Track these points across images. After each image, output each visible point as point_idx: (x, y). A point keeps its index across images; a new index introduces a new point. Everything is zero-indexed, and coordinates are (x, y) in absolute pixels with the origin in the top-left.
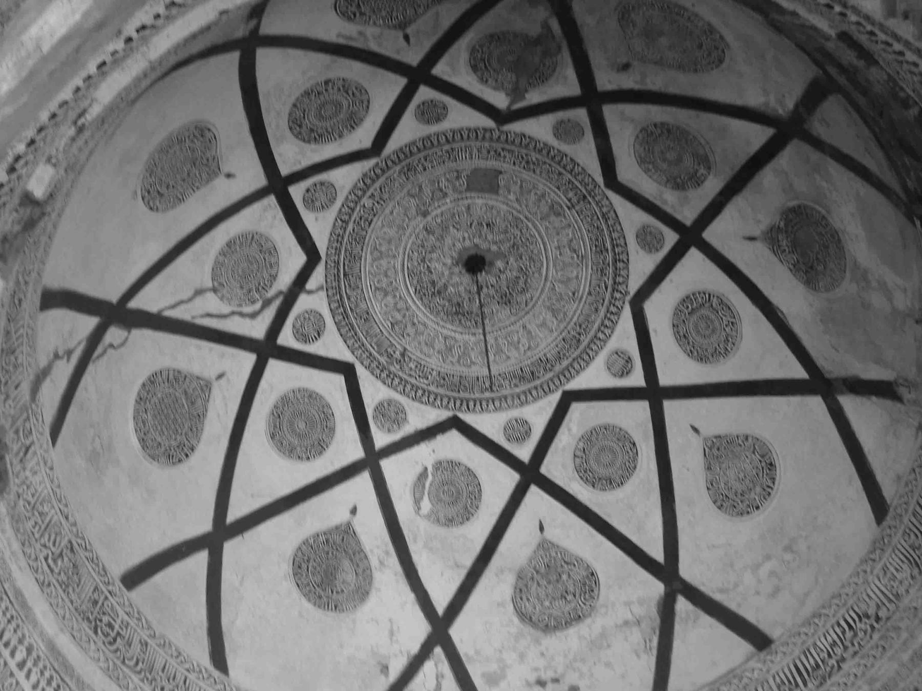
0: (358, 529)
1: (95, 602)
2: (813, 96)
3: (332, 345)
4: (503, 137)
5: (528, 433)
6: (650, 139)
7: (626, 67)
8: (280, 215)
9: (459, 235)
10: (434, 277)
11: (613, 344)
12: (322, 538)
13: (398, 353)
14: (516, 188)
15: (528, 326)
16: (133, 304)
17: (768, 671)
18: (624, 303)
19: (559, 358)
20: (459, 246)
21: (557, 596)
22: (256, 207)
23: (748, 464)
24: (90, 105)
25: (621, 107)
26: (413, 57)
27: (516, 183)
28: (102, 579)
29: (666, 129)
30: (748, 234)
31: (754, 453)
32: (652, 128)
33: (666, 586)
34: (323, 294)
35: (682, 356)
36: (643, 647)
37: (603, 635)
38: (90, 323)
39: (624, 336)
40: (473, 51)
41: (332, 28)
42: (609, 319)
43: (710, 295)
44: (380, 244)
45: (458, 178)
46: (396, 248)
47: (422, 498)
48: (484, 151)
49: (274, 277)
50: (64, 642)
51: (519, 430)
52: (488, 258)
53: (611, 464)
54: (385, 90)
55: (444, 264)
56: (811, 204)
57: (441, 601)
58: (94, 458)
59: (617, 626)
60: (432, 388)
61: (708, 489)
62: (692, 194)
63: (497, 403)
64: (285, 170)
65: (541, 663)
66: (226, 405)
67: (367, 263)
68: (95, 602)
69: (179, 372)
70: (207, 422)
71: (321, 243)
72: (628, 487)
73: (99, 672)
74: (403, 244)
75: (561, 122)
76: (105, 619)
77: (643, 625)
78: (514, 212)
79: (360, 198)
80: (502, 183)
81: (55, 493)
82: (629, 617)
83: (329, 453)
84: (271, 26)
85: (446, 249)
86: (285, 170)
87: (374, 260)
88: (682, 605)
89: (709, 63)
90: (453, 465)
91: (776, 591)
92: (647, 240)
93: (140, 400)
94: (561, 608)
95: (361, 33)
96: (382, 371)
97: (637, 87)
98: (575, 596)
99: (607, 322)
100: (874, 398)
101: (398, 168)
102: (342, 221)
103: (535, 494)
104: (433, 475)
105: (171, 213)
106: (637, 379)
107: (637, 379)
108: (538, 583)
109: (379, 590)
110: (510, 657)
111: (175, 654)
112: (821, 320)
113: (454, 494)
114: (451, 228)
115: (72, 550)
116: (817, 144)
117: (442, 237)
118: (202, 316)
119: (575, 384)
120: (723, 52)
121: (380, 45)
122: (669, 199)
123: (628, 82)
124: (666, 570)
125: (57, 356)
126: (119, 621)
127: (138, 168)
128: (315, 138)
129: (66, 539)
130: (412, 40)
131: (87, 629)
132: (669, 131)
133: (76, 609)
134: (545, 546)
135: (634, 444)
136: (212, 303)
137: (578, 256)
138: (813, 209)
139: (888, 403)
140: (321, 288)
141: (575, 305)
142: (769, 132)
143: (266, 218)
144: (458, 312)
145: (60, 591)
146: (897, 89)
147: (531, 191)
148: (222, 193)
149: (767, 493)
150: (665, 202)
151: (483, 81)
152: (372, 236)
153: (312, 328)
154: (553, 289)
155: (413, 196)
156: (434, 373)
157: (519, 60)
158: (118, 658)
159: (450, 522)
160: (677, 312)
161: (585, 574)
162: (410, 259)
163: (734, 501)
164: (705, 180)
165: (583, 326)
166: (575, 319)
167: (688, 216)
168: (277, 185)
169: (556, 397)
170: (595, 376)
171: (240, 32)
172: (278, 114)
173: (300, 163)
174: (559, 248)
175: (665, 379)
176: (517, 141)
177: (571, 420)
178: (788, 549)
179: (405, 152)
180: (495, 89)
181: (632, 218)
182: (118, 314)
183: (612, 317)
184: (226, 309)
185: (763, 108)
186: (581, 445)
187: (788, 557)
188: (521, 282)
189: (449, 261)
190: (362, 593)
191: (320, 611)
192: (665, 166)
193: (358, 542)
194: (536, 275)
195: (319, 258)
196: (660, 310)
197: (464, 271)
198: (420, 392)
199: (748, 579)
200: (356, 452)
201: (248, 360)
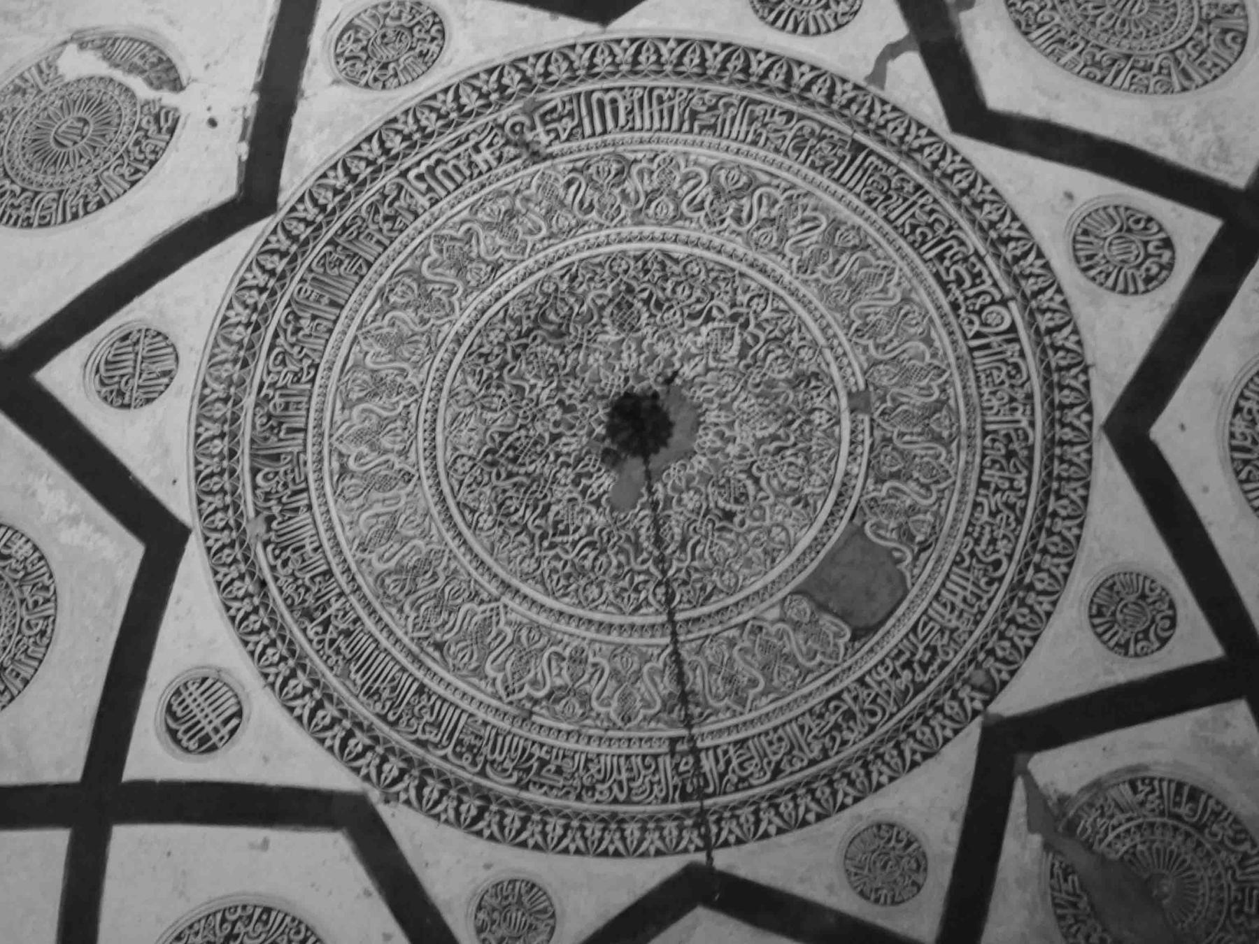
4: (951, 707)
5: (118, 398)
8: (1169, 153)
9: (744, 436)
11: (263, 706)
13: (545, 139)
14: (795, 643)
15: (403, 491)
18: (367, 778)
19: (284, 546)
20: (711, 417)
34: (859, 71)
39: (275, 748)
45: (906, 535)
47: (107, 58)
49: (1024, 28)
52: (635, 466)
55: (687, 357)
60: (388, 179)
63: (240, 334)
67: (839, 201)
74: (807, 298)
75: (921, 864)
78: (731, 600)
80: (826, 620)
85: (728, 383)
87: (836, 224)
90: (140, 163)
96: (525, 79)
99: (330, 711)
101: (1037, 437)
102: (1010, 239)
106: (150, 757)
107: (150, 757)
119: (193, 567)
137: (536, 702)
140: (878, 76)
141: (406, 640)
144: (545, 322)
151: (1136, 779)
154: (474, 596)
156: (424, 201)
162: (764, 294)
165: (342, 642)
166: (369, 623)
169: (180, 502)
174: (578, 659)
175: (126, 841)
176: (924, 733)
177: (100, 529)
179: (1065, 488)
180: (1097, 786)
183: (339, 732)
186: (20, 549)
189: (687, 371)
194: (530, 565)
195: (958, 126)
197: (638, 389)
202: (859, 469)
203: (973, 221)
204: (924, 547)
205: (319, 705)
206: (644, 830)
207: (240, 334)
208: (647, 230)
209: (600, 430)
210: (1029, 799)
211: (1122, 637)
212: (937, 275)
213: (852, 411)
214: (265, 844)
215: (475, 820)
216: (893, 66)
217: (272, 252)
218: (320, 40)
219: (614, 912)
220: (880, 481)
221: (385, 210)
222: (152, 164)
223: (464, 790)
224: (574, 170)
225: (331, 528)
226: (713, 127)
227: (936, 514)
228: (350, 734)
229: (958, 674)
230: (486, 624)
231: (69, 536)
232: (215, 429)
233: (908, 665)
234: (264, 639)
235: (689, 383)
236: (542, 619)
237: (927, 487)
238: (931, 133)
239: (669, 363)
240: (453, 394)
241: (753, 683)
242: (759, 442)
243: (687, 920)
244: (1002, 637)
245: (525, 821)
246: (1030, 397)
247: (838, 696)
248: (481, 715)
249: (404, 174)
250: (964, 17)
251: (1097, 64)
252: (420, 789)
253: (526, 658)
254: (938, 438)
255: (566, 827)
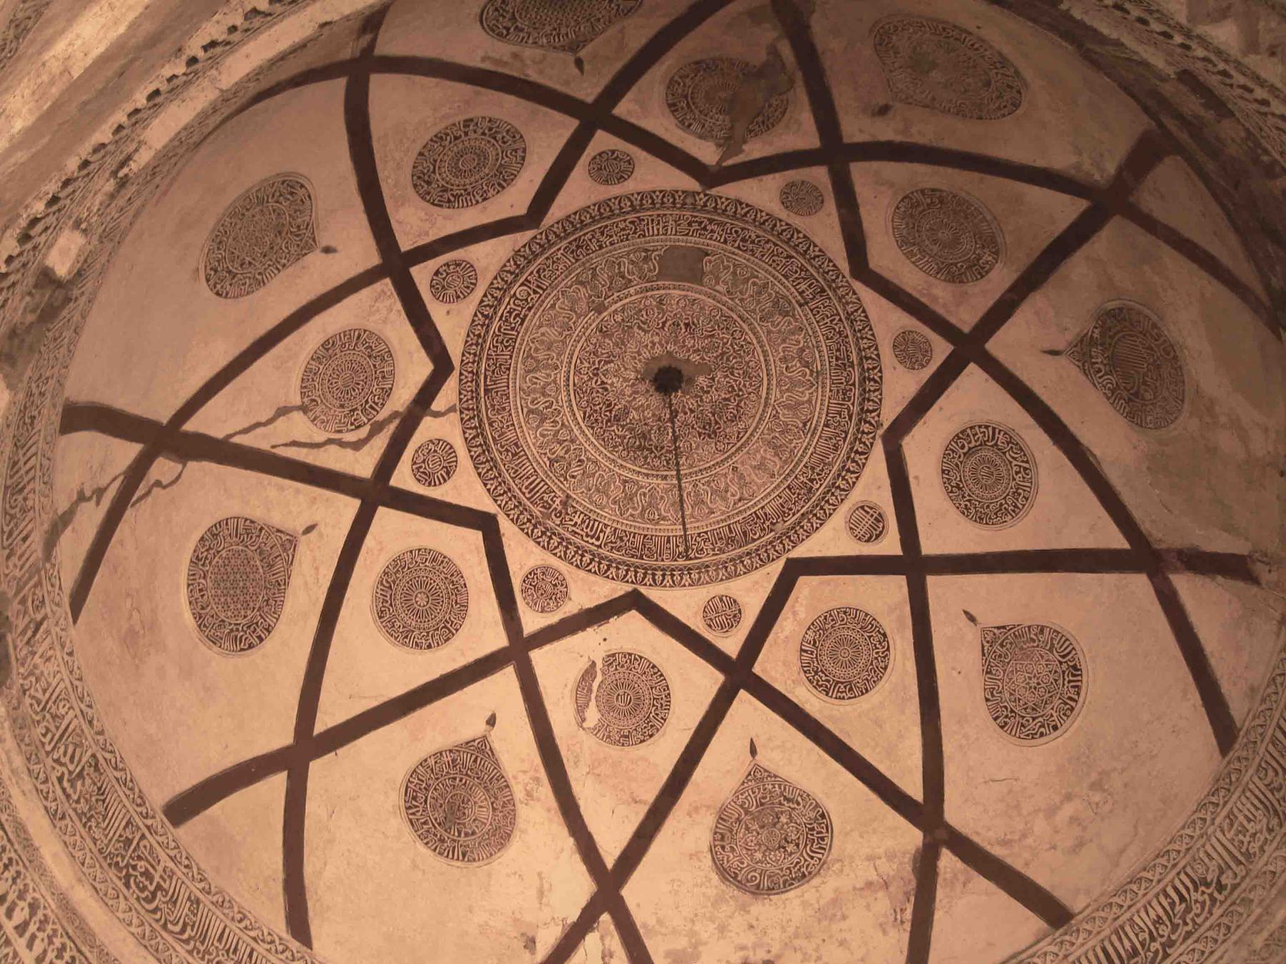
0: (496, 746)
1: (128, 842)
2: (1143, 157)
3: (465, 488)
4: (711, 205)
5: (737, 617)
6: (916, 212)
7: (883, 110)
8: (399, 306)
9: (647, 339)
10: (611, 396)
11: (856, 496)
12: (447, 758)
13: (558, 501)
16: (190, 426)
17: (1066, 957)
18: (874, 438)
19: (783, 513)
20: (646, 354)
21: (772, 845)
22: (365, 294)
23: (1043, 666)
24: (136, 150)
25: (875, 165)
26: (588, 91)
27: (727, 268)
28: (139, 809)
29: (937, 198)
30: (1048, 346)
31: (1051, 650)
32: (919, 196)
33: (925, 836)
34: (455, 417)
35: (954, 514)
36: (892, 918)
37: (834, 902)
38: (128, 451)
39: (873, 484)
40: (671, 84)
41: (475, 47)
42: (853, 461)
43: (994, 429)
44: (537, 350)
45: (646, 259)
46: (559, 355)
48: (684, 224)
49: (388, 393)
50: (82, 897)
51: (725, 613)
52: (686, 371)
53: (852, 663)
54: (546, 136)
55: (626, 380)
56: (1137, 306)
57: (610, 852)
58: (130, 638)
59: (854, 888)
60: (603, 552)
61: (987, 700)
62: (973, 288)
63: (695, 576)
64: (406, 243)
65: (748, 939)
66: (317, 569)
67: (517, 378)
68: (128, 842)
69: (252, 522)
70: (289, 592)
71: (455, 348)
72: (874, 697)
73: (131, 940)
74: (571, 352)
75: (792, 185)
76: (142, 865)
77: (892, 889)
79: (510, 285)
80: (707, 268)
81: (75, 688)
82: (873, 876)
83: (457, 641)
84: (391, 43)
86: (406, 243)
88: (947, 861)
89: (999, 108)
91: (1080, 844)
92: (909, 351)
93: (196, 560)
94: (778, 863)
95: (515, 56)
96: (535, 526)
97: (898, 138)
98: (797, 845)
100: (1220, 579)
101: (564, 243)
102: (484, 316)
103: (745, 705)
104: (603, 674)
105: (245, 302)
106: (890, 545)
107: (890, 545)
108: (747, 829)
109: (524, 832)
110: (706, 930)
111: (238, 916)
112: (1149, 468)
113: (631, 700)
114: (635, 329)
115: (96, 768)
116: (1148, 224)
117: (623, 343)
118: (285, 445)
119: (801, 551)
120: (1019, 92)
121: (541, 72)
122: (940, 295)
123: (886, 131)
124: (925, 812)
125: (82, 498)
126: (160, 868)
127: (200, 237)
128: (449, 201)
129: (89, 753)
130: (587, 67)
131: (115, 879)
132: (941, 202)
133: (100, 851)
134: (757, 775)
135: (885, 635)
136: (299, 427)
137: (811, 371)
138: (1139, 313)
139: (1240, 584)
140: (452, 409)
142: (1082, 204)
143: (378, 311)
144: (641, 446)
145: (79, 826)
146: (1260, 151)
147: (748, 279)
148: (317, 274)
149: (1069, 707)
150: (935, 299)
152: (526, 337)
153: (439, 464)
155: (582, 283)
157: (739, 98)
158: (157, 921)
159: (625, 739)
160: (948, 452)
161: (812, 815)
162: (578, 371)
163: (1022, 718)
164: (991, 269)
165: (817, 470)
166: (805, 460)
167: (966, 319)
168: (395, 265)
169: (777, 568)
170: (832, 540)
171: (347, 54)
172: (399, 166)
173: (427, 234)
174: (783, 360)
175: (930, 546)
178: (1096, 786)
179: (572, 223)
180: (700, 137)
181: (887, 321)
182: (170, 440)
184: (320, 437)
185: (1073, 172)
187: (1097, 797)
188: (733, 405)
189: (633, 375)
190: (501, 836)
191: (442, 859)
192: (936, 248)
193: (497, 764)
195: (453, 369)
196: (924, 449)
197: (652, 390)
198: (588, 557)
199: (1040, 825)
200: (497, 639)
201: (349, 507)
202: (632, 290)
203: (487, 332)
204: (646, 251)
205: (848, 471)
206: (848, 303)
207: (695, 576)
208: (577, 433)
209: (679, 394)
210: (730, 157)
211: (623, 165)
212: (522, 324)
213: (606, 309)
214: (916, 477)
215: (876, 382)
216: (443, 409)
217: (654, 580)
218: (553, 618)
219: (891, 305)
220: (630, 281)
221: (619, 543)
222: (630, 654)
223: (864, 390)
224: (566, 479)
225: (769, 494)
226: (516, 444)
227: (628, 254)
228: (857, 452)
229: (694, 209)
230: (788, 407)
231: (802, 615)
232: (740, 567)
233: (705, 229)
234: (827, 506)
235: (637, 371)
236: (774, 382)
237: (619, 264)
238: (461, 374)
239: (633, 385)
240: (691, 466)
241: (754, 284)
242: (646, 332)
243: (878, 270)
244: (663, 203)
245: (867, 359)
246: (547, 258)
247: (738, 248)
248: (828, 394)
249: (600, 546)
250: (401, 410)
251: (383, 360)
252: (872, 412)
253: (795, 383)
254: (594, 276)
255: (862, 338)
